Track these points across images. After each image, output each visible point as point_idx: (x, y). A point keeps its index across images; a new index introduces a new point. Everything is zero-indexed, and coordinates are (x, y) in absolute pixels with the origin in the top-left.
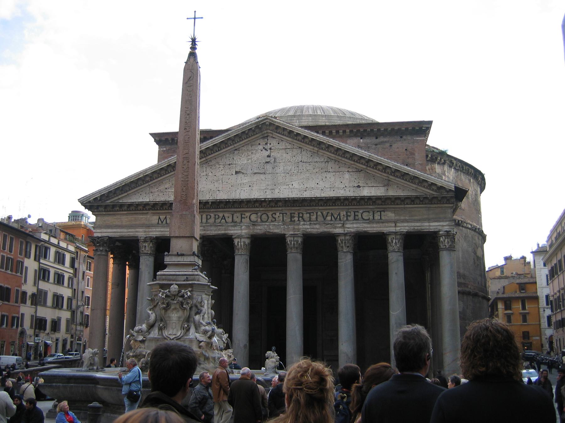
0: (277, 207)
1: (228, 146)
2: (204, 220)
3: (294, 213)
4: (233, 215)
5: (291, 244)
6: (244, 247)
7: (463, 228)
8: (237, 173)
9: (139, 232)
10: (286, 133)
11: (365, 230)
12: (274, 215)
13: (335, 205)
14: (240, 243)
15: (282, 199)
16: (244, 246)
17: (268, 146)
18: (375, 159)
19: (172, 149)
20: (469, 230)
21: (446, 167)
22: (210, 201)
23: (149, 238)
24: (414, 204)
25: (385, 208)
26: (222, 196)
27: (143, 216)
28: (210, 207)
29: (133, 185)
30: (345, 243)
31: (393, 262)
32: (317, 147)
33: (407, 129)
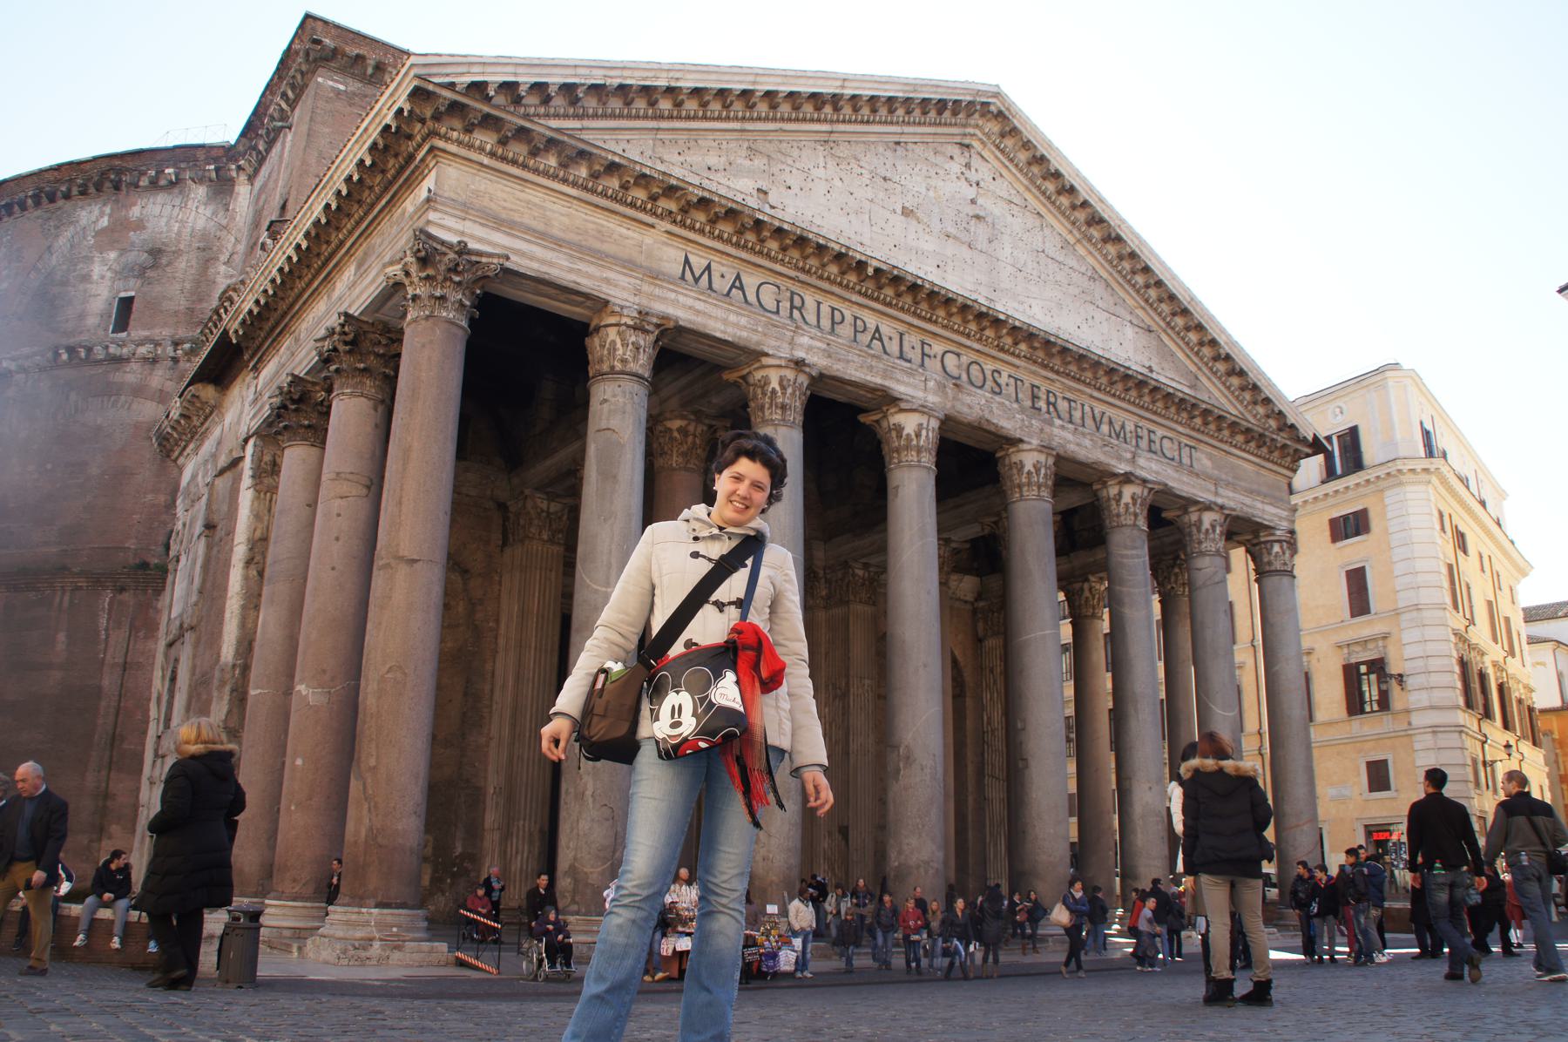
0: (1013, 354)
1: (891, 123)
2: (826, 323)
3: (1038, 388)
4: (901, 335)
5: (1038, 475)
9: (616, 286)
10: (1023, 156)
12: (996, 375)
14: (924, 433)
15: (1042, 333)
17: (973, 176)
19: (366, 96)
22: (875, 263)
23: (655, 320)
27: (630, 233)
28: (855, 284)
29: (615, 104)
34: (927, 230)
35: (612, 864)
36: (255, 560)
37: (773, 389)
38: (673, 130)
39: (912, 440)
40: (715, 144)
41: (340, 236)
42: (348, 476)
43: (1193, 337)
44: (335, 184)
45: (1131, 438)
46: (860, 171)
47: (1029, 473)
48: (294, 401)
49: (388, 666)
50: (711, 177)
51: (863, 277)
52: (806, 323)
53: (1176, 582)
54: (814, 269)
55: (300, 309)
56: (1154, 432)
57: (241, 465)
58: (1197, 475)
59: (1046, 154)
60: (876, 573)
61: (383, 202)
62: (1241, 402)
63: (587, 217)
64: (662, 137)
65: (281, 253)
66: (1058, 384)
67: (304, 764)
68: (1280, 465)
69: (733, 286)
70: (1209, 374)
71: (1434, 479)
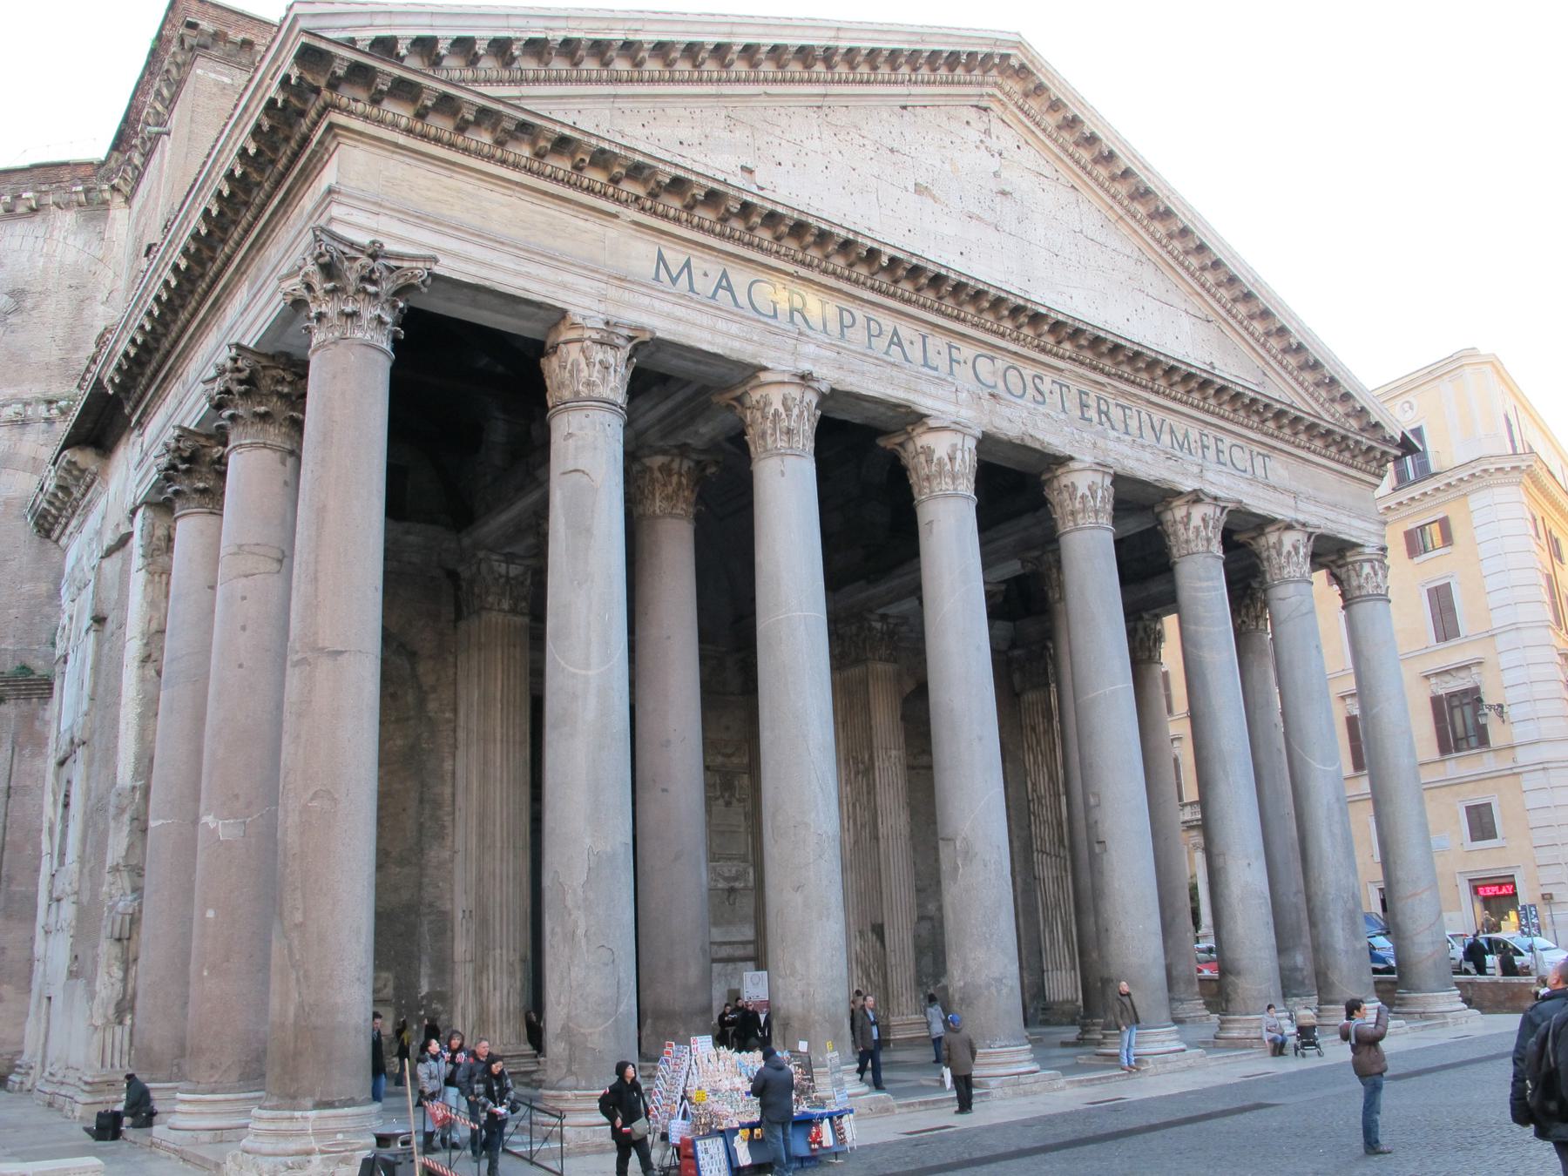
0: (1056, 355)
3: (1087, 394)
4: (924, 337)
9: (575, 291)
10: (1051, 121)
12: (1037, 381)
13: (1186, 403)
14: (959, 455)
15: (1089, 328)
18: (1263, 297)
22: (890, 251)
23: (626, 332)
27: (589, 225)
28: (866, 277)
29: (559, 65)
31: (1307, 613)
34: (946, 210)
35: (616, 1021)
36: (153, 658)
37: (776, 413)
39: (946, 464)
41: (226, 249)
42: (256, 549)
44: (213, 182)
46: (862, 141)
48: (184, 460)
49: (311, 793)
50: (684, 154)
51: (876, 267)
52: (811, 328)
53: (1247, 615)
54: (816, 261)
55: (186, 346)
57: (129, 544)
58: (1275, 488)
60: (896, 625)
61: (276, 202)
62: (1317, 400)
63: (533, 207)
64: (621, 105)
65: (156, 277)
66: (1109, 389)
67: (216, 916)
68: (1364, 471)
69: (719, 286)
71: (1526, 479)
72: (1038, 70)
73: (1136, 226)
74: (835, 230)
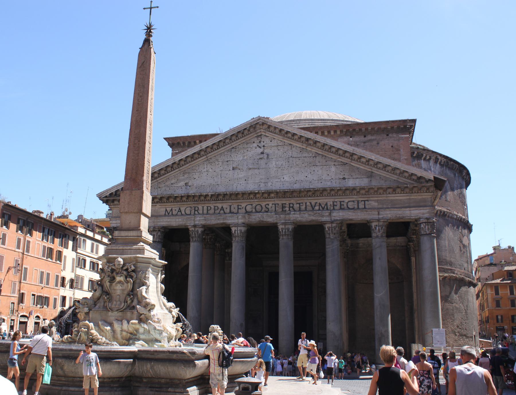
0: (270, 198)
1: (226, 145)
2: (205, 212)
3: (285, 204)
4: (230, 206)
6: (240, 236)
7: (449, 219)
8: (234, 169)
11: (351, 218)
13: (323, 196)
14: (236, 232)
15: (273, 191)
16: (240, 235)
18: (358, 153)
20: (454, 220)
21: (432, 162)
22: (210, 194)
23: (157, 228)
24: (396, 193)
25: (368, 197)
26: (221, 189)
30: (332, 230)
31: (377, 248)
32: (305, 143)
33: (392, 128)
34: (242, 170)
38: (161, 179)
40: (173, 177)
43: (363, 160)
45: (331, 207)
47: (280, 232)
56: (343, 201)
58: (367, 211)
59: (281, 128)
62: (396, 174)
68: (421, 193)
69: (178, 211)
70: (377, 170)
72: (267, 122)
73: (312, 147)
74: (196, 194)
